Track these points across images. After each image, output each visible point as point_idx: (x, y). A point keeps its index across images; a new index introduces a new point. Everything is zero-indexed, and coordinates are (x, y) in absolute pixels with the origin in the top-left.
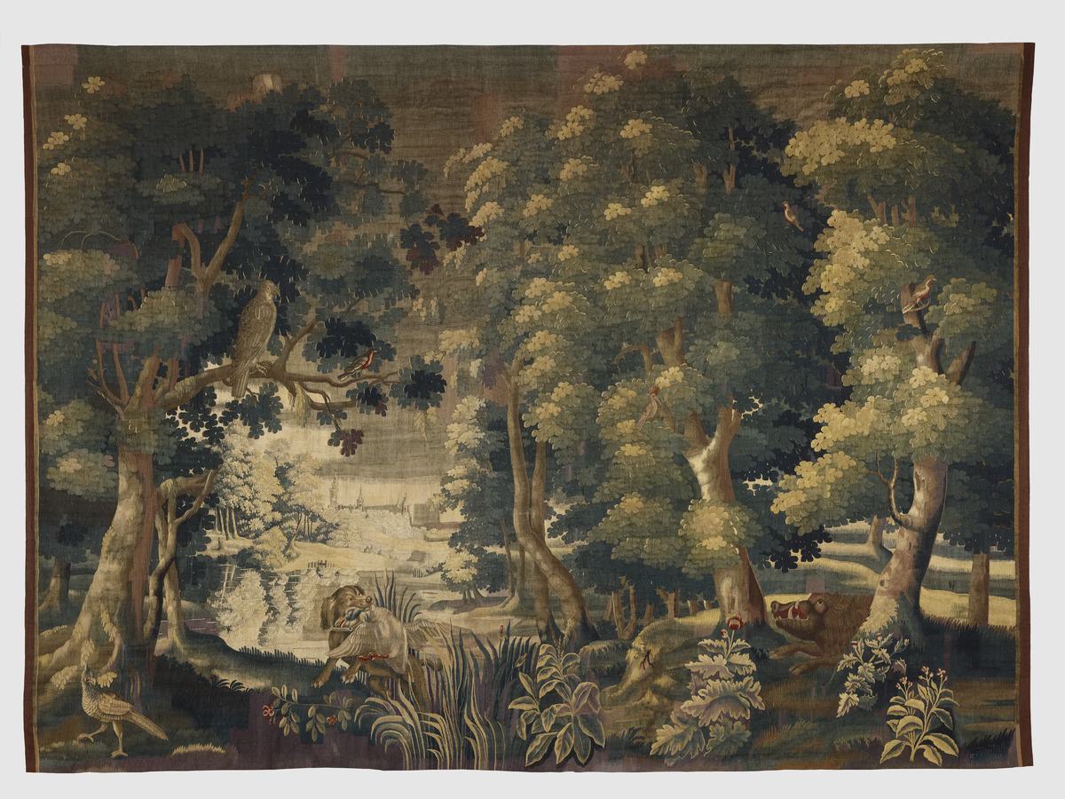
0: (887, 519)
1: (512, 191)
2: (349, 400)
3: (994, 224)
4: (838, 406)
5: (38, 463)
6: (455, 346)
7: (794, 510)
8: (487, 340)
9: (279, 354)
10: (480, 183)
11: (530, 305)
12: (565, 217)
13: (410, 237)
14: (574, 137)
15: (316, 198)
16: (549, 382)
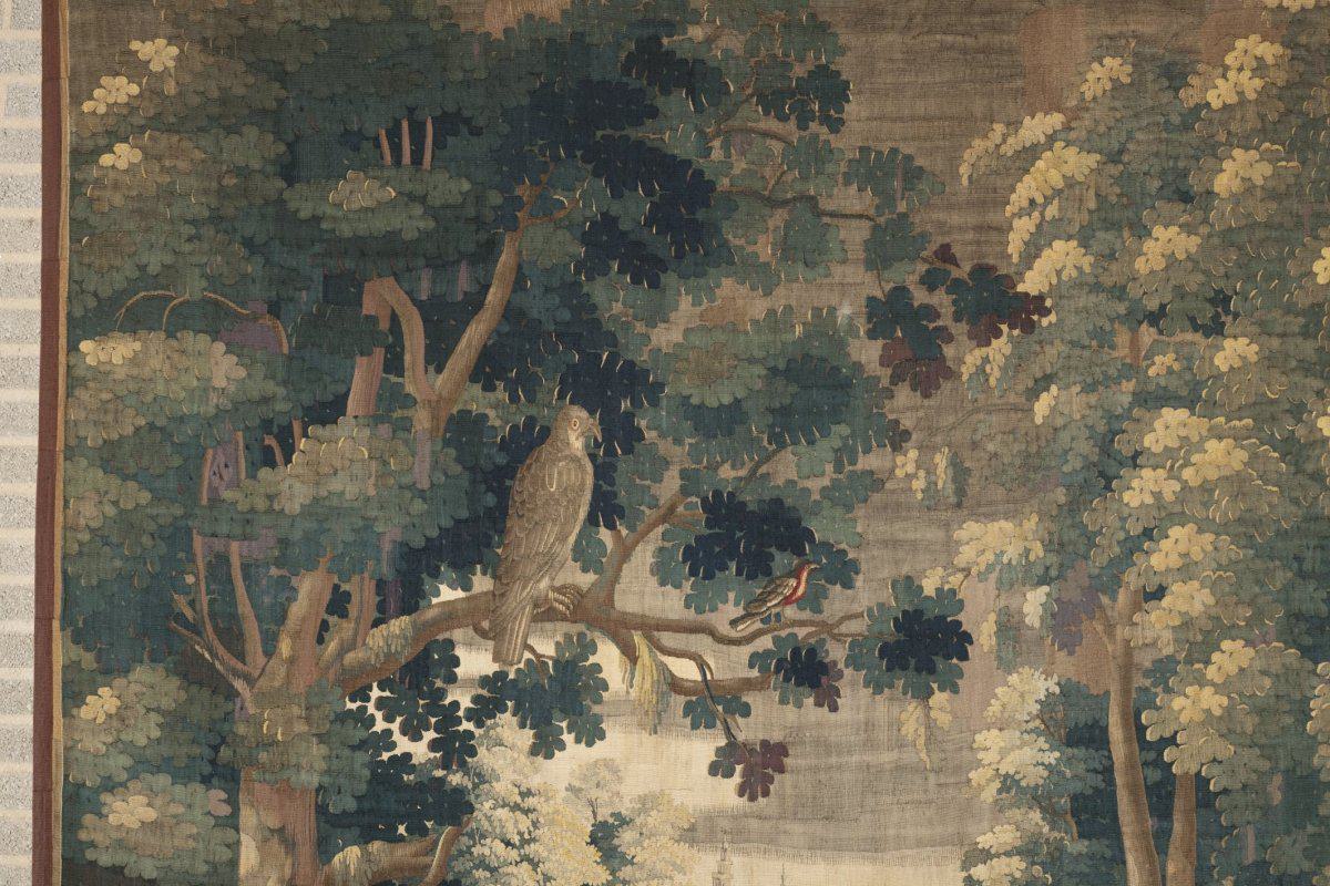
1: (1111, 218)
2: (755, 673)
5: (62, 805)
6: (989, 557)
8: (1061, 544)
9: (599, 570)
10: (1040, 200)
12: (1227, 276)
13: (889, 314)
14: (1243, 101)
15: (679, 225)
16: (1200, 642)
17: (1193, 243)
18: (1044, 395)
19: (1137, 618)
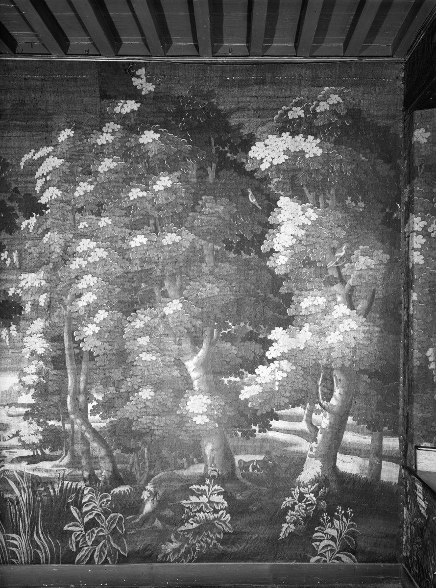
0: (316, 405)
1: (67, 180)
4: (284, 329)
6: (29, 284)
7: (254, 398)
10: (45, 174)
11: (80, 257)
12: (102, 198)
17: (92, 188)
18: (46, 235)
19: (73, 303)
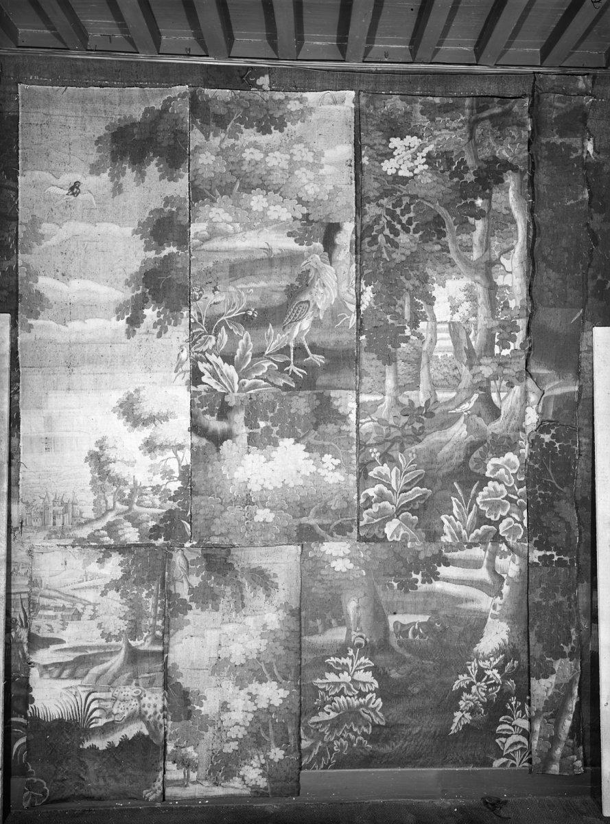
0: (500, 545)
3: (599, 277)
